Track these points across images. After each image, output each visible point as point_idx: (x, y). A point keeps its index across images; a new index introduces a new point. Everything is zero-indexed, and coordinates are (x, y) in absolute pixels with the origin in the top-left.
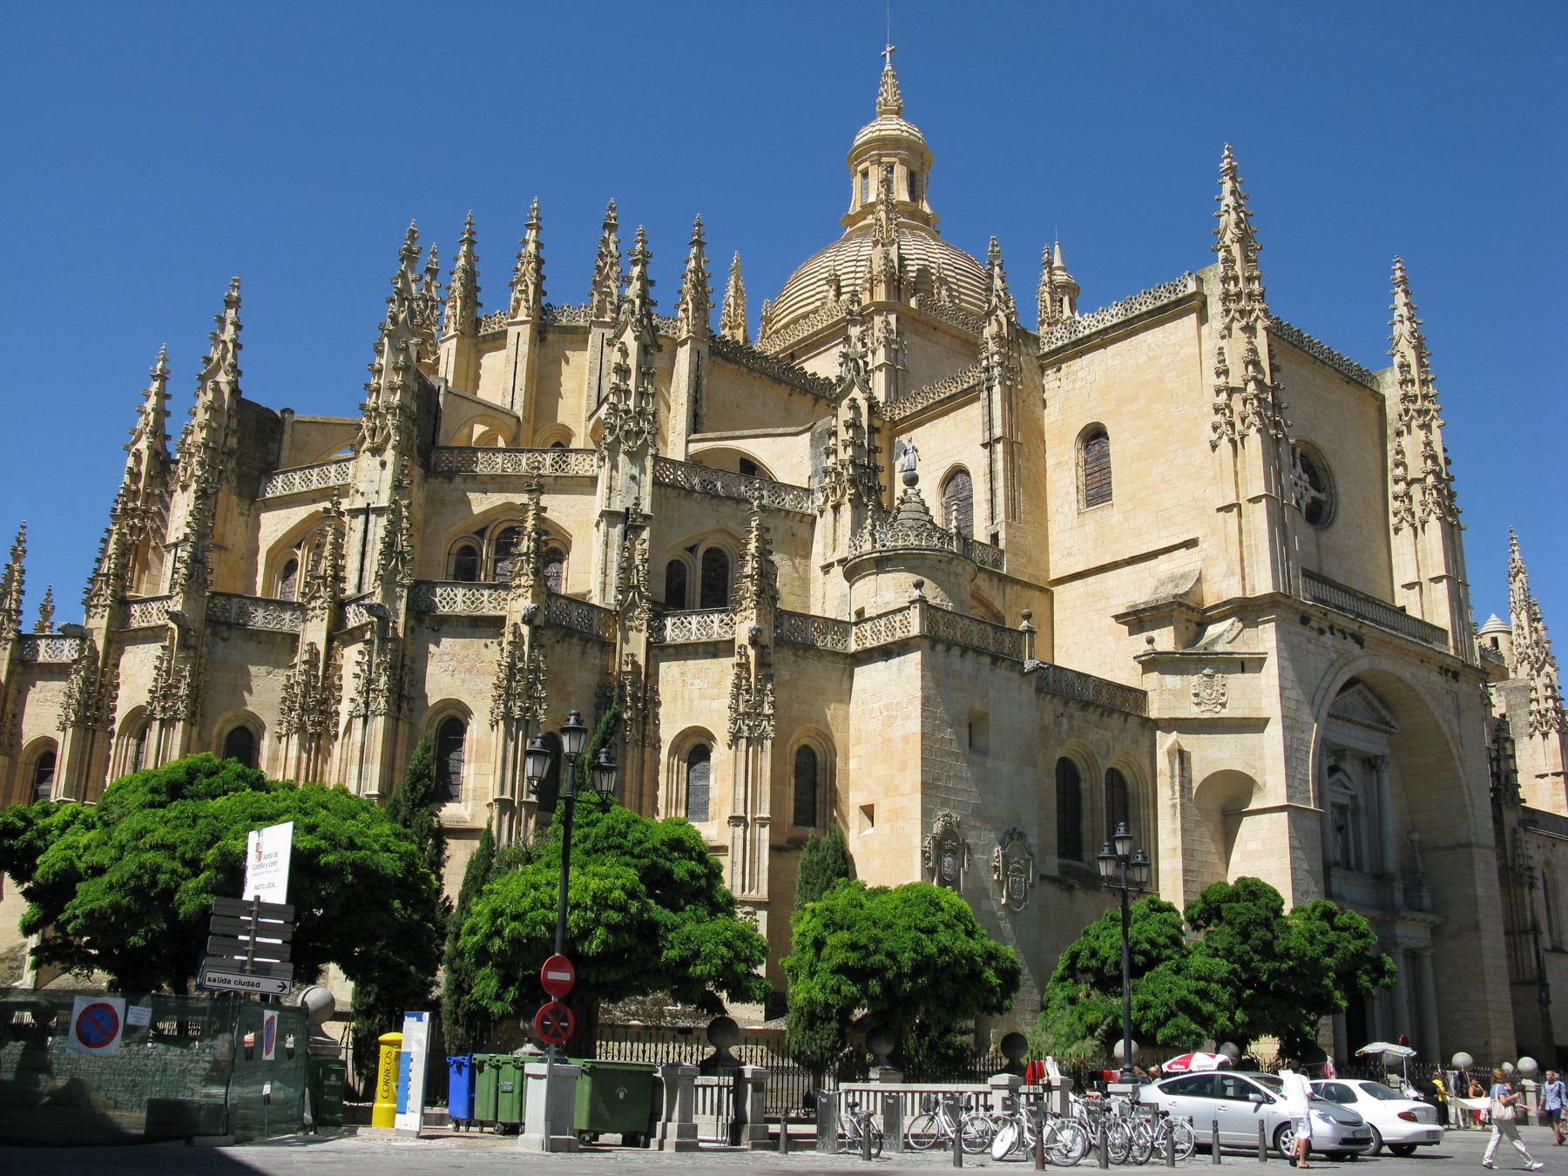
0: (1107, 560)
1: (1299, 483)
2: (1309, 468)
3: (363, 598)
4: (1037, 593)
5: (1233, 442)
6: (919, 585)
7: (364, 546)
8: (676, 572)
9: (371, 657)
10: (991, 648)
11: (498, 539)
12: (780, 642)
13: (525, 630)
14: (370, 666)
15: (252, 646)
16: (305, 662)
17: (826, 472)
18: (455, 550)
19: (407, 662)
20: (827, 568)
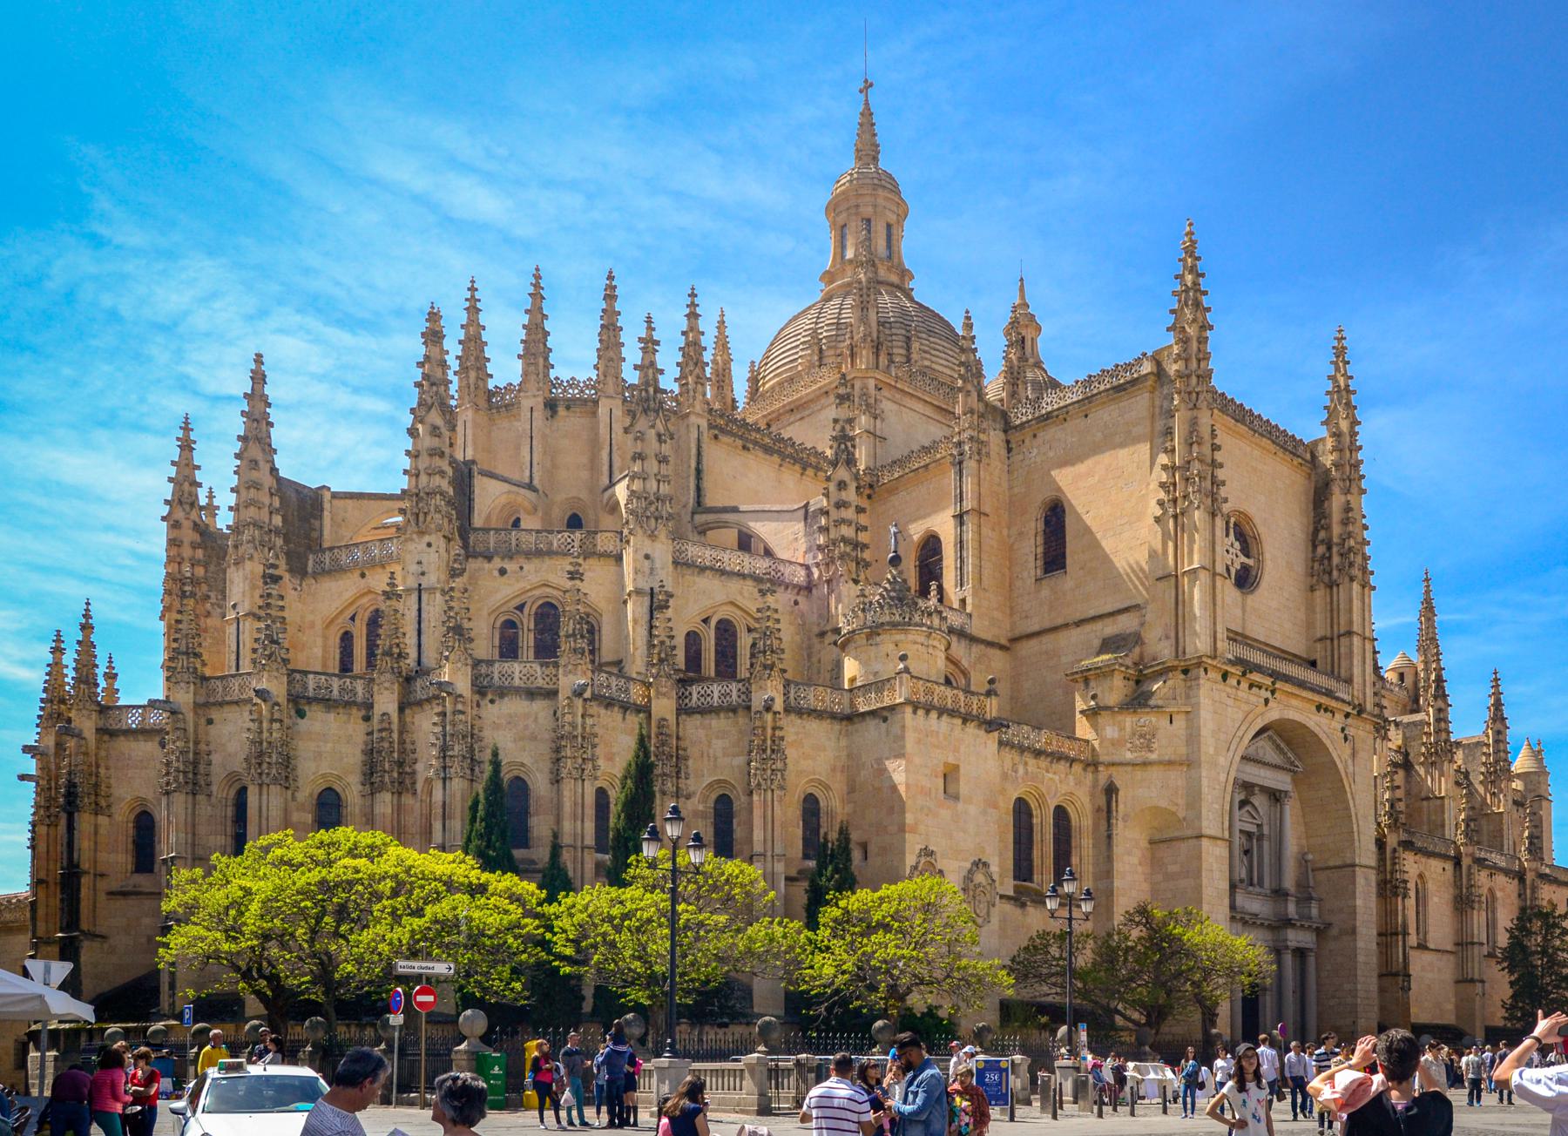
0: (1060, 621)
1: (1231, 550)
2: (1241, 536)
3: (427, 673)
4: (998, 652)
5: (1175, 517)
6: (903, 658)
7: (419, 623)
8: (693, 639)
9: (444, 727)
10: (962, 710)
11: (536, 614)
12: (788, 710)
13: (579, 702)
14: (445, 736)
15: (332, 716)
16: (380, 731)
17: (819, 548)
18: (498, 624)
19: (476, 731)
20: (822, 634)
